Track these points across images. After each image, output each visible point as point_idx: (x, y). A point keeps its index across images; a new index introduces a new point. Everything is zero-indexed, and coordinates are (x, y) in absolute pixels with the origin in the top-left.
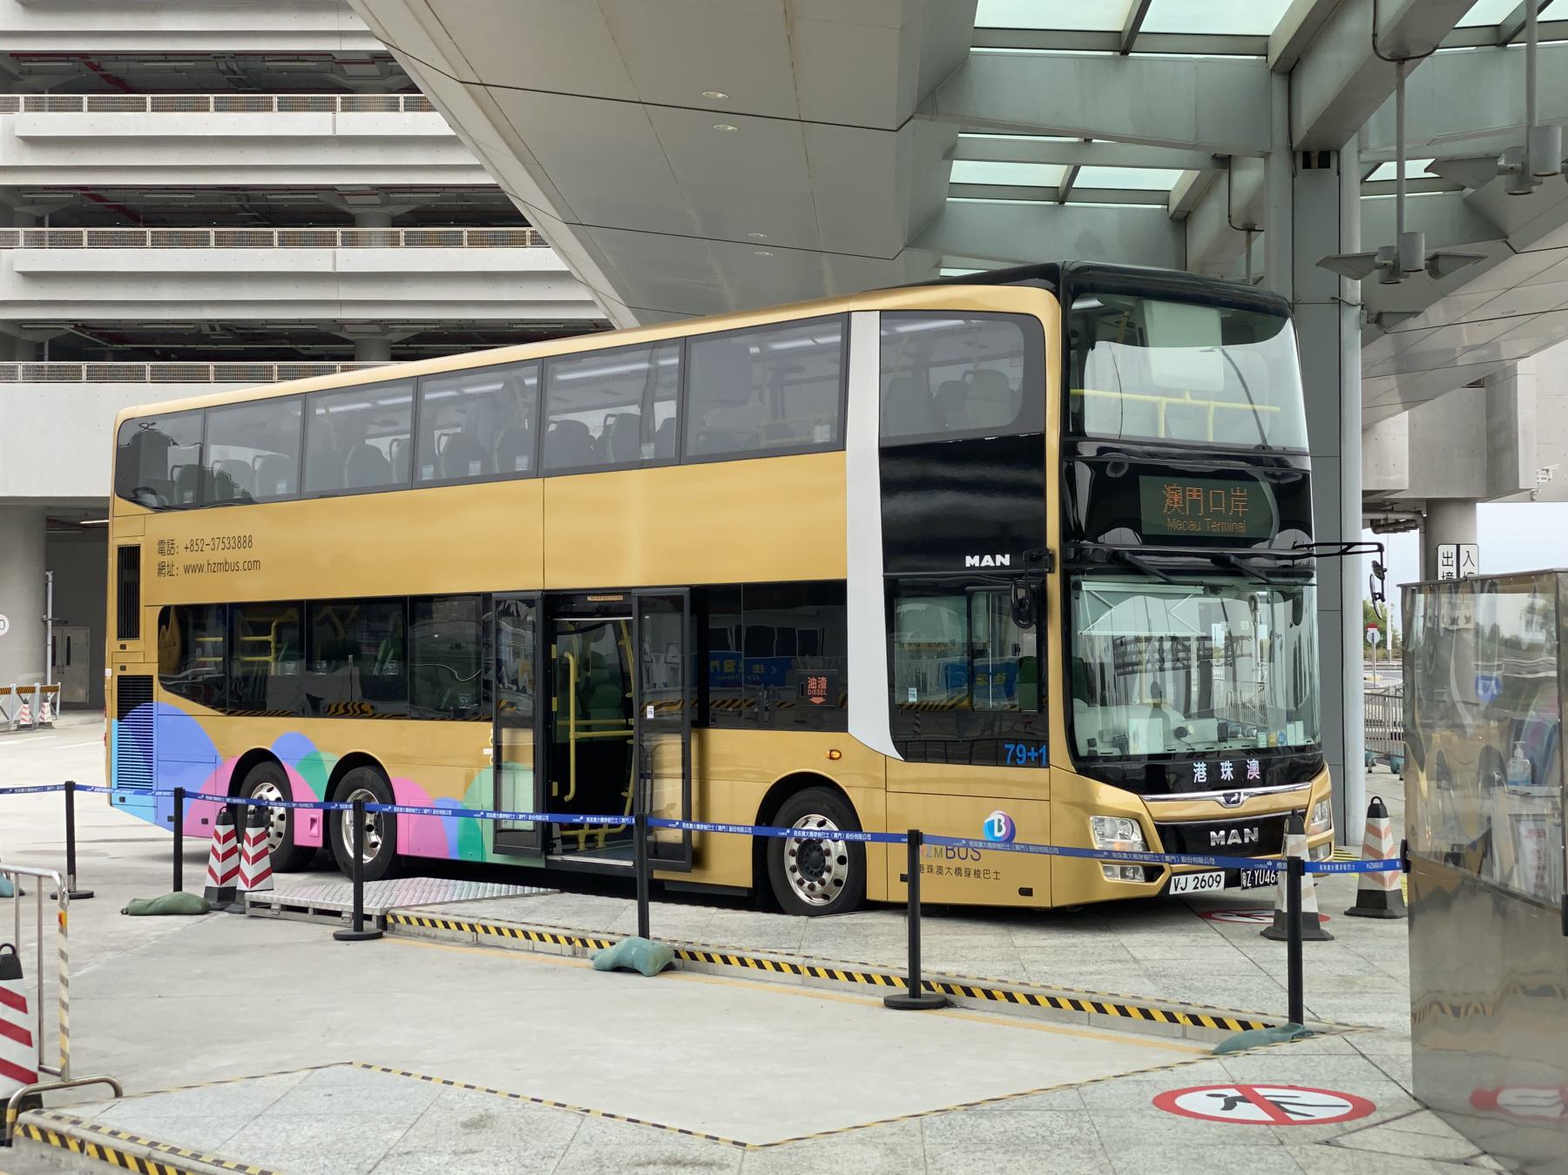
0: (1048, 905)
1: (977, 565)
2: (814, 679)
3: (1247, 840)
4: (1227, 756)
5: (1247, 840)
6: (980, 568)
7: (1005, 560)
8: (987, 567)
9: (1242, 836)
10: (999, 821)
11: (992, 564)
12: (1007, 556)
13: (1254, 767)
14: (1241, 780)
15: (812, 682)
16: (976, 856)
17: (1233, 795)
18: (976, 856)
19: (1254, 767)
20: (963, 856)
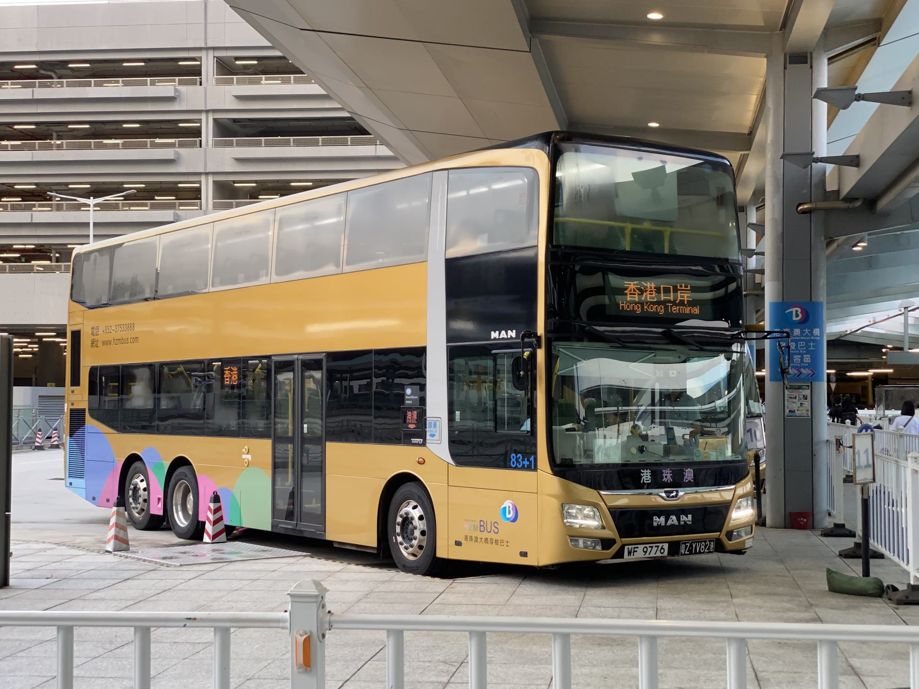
0: (536, 564)
1: (497, 337)
4: (667, 465)
5: (682, 523)
6: (499, 339)
7: (512, 334)
8: (503, 339)
9: (679, 520)
10: (509, 507)
11: (506, 337)
12: (514, 331)
13: (689, 474)
15: (409, 414)
16: (496, 531)
17: (672, 492)
18: (496, 531)
19: (689, 474)
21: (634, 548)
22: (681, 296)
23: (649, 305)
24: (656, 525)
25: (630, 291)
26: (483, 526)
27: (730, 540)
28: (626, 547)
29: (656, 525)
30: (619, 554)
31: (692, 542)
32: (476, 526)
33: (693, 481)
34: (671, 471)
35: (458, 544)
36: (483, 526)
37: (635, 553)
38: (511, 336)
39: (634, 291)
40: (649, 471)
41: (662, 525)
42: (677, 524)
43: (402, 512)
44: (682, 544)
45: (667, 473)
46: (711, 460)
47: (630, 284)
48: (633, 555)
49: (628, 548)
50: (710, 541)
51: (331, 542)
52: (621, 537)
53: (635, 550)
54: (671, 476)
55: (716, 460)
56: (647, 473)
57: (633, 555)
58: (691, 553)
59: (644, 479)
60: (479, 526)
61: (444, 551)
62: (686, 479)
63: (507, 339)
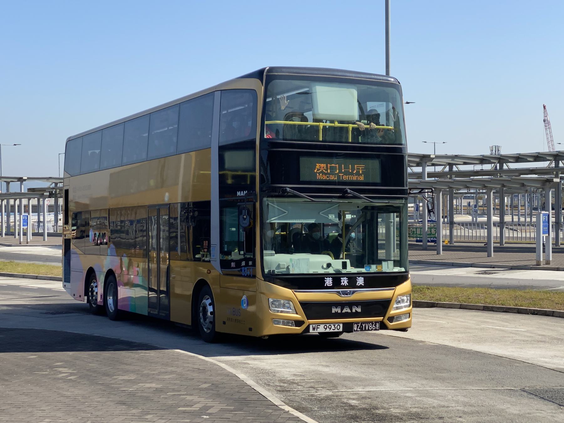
5: (354, 311)
9: (351, 310)
13: (360, 281)
19: (360, 281)
29: (334, 312)
33: (363, 285)
34: (347, 279)
37: (318, 329)
41: (338, 312)
44: (354, 324)
45: (345, 280)
48: (317, 330)
49: (313, 326)
53: (318, 327)
56: (329, 280)
57: (317, 330)
62: (358, 284)
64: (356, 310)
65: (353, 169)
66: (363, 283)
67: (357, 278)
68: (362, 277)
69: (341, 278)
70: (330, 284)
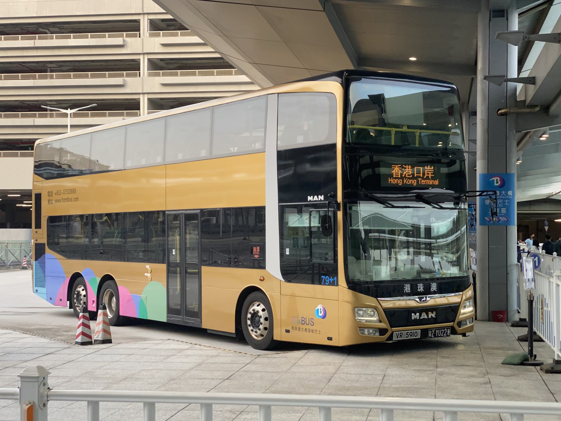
2: (255, 248)
3: (430, 317)
5: (430, 317)
7: (322, 198)
8: (316, 201)
9: (428, 315)
10: (321, 309)
11: (317, 199)
12: (323, 196)
13: (434, 287)
14: (427, 291)
15: (255, 249)
16: (312, 324)
17: (423, 298)
19: (434, 287)
20: (307, 324)
21: (400, 333)
22: (428, 174)
23: (407, 179)
24: (414, 319)
25: (396, 171)
26: (304, 321)
27: (460, 327)
28: (394, 333)
29: (414, 319)
30: (391, 337)
31: (435, 330)
32: (299, 321)
33: (436, 290)
34: (423, 285)
35: (288, 331)
36: (304, 321)
38: (321, 199)
39: (398, 171)
40: (409, 285)
42: (426, 317)
43: (251, 310)
45: (421, 286)
46: (447, 276)
47: (395, 167)
50: (447, 329)
51: (206, 330)
52: (391, 327)
54: (423, 288)
55: (450, 276)
56: (408, 286)
58: (434, 337)
59: (406, 290)
60: (301, 322)
61: (279, 335)
62: (432, 290)
63: (318, 201)
64: (431, 316)
65: (424, 174)
66: (436, 289)
67: (431, 283)
68: (435, 283)
69: (418, 285)
70: (409, 290)
